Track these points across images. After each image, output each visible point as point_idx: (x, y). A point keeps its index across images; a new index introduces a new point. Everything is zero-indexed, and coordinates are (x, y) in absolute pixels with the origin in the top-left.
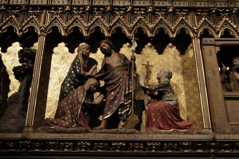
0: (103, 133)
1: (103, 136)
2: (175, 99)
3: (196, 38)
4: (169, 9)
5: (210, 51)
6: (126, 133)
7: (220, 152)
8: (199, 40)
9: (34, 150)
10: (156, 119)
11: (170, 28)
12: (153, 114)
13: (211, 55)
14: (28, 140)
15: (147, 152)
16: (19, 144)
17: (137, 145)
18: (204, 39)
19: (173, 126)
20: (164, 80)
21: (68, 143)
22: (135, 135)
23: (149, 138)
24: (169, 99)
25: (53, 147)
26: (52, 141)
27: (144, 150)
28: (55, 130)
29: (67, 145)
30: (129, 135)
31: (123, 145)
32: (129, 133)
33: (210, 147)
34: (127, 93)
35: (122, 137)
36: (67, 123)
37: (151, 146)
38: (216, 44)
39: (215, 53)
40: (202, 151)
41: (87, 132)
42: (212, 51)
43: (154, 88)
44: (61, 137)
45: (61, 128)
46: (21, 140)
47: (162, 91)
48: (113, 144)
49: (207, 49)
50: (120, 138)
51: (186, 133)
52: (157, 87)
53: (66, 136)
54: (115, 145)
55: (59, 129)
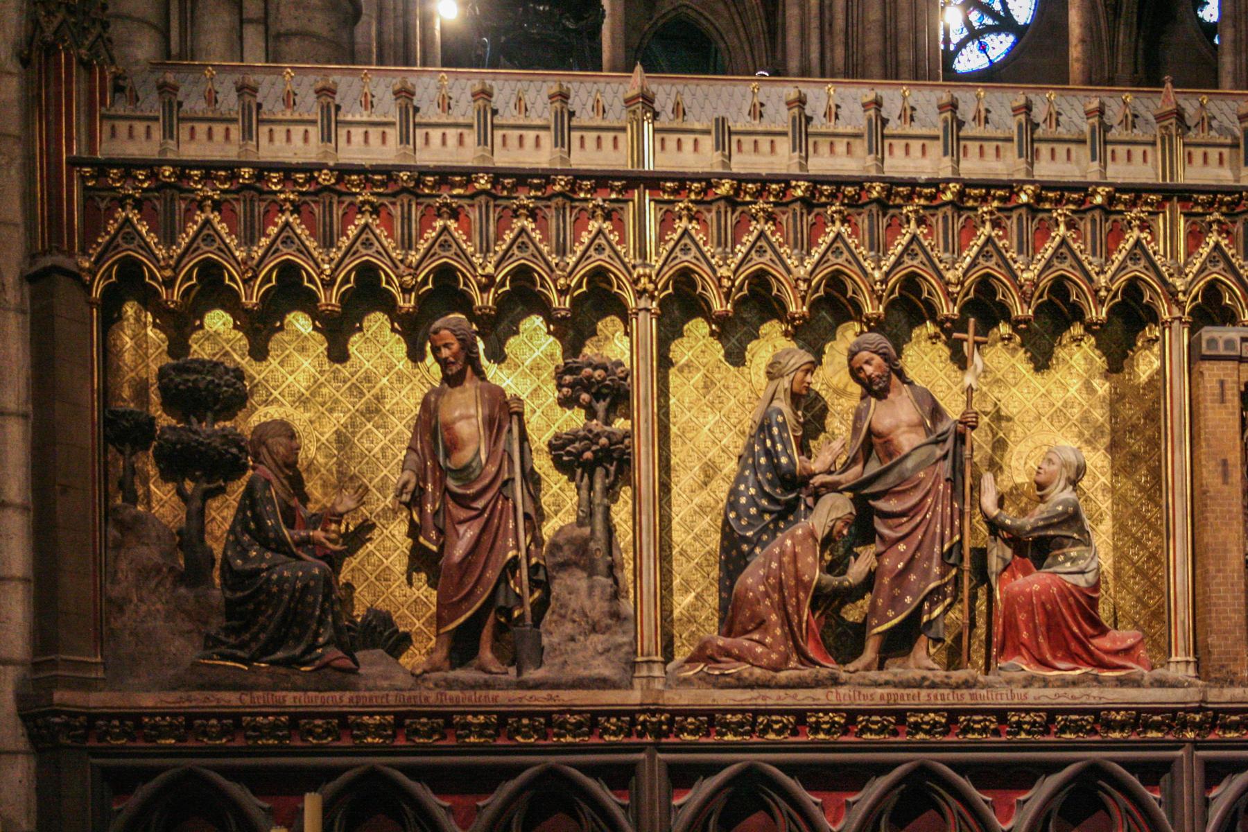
0: (877, 684)
1: (882, 697)
2: (1094, 565)
3: (1176, 323)
4: (1095, 193)
5: (1222, 383)
6: (947, 686)
7: (1211, 737)
8: (1186, 330)
9: (677, 736)
10: (1034, 634)
11: (1091, 280)
12: (1022, 617)
13: (1223, 401)
14: (662, 712)
15: (1003, 739)
16: (633, 722)
17: (979, 722)
18: (1208, 333)
19: (1082, 659)
20: (1060, 495)
21: (779, 718)
22: (974, 691)
23: (1016, 701)
24: (1074, 569)
25: (735, 728)
26: (734, 712)
27: (996, 732)
28: (739, 679)
29: (777, 722)
30: (959, 692)
31: (940, 723)
32: (958, 687)
33: (1184, 725)
34: (946, 547)
35: (936, 697)
36: (774, 656)
37: (1019, 724)
38: (1244, 355)
39: (1236, 392)
40: (1160, 735)
41: (835, 681)
42: (1227, 386)
43: (1028, 528)
44: (760, 702)
45: (758, 672)
46: (643, 712)
47: (1053, 537)
48: (912, 719)
49: (1212, 373)
50: (933, 701)
51: (1121, 682)
52: (1041, 523)
53: (773, 698)
54: (916, 723)
55: (751, 674)
